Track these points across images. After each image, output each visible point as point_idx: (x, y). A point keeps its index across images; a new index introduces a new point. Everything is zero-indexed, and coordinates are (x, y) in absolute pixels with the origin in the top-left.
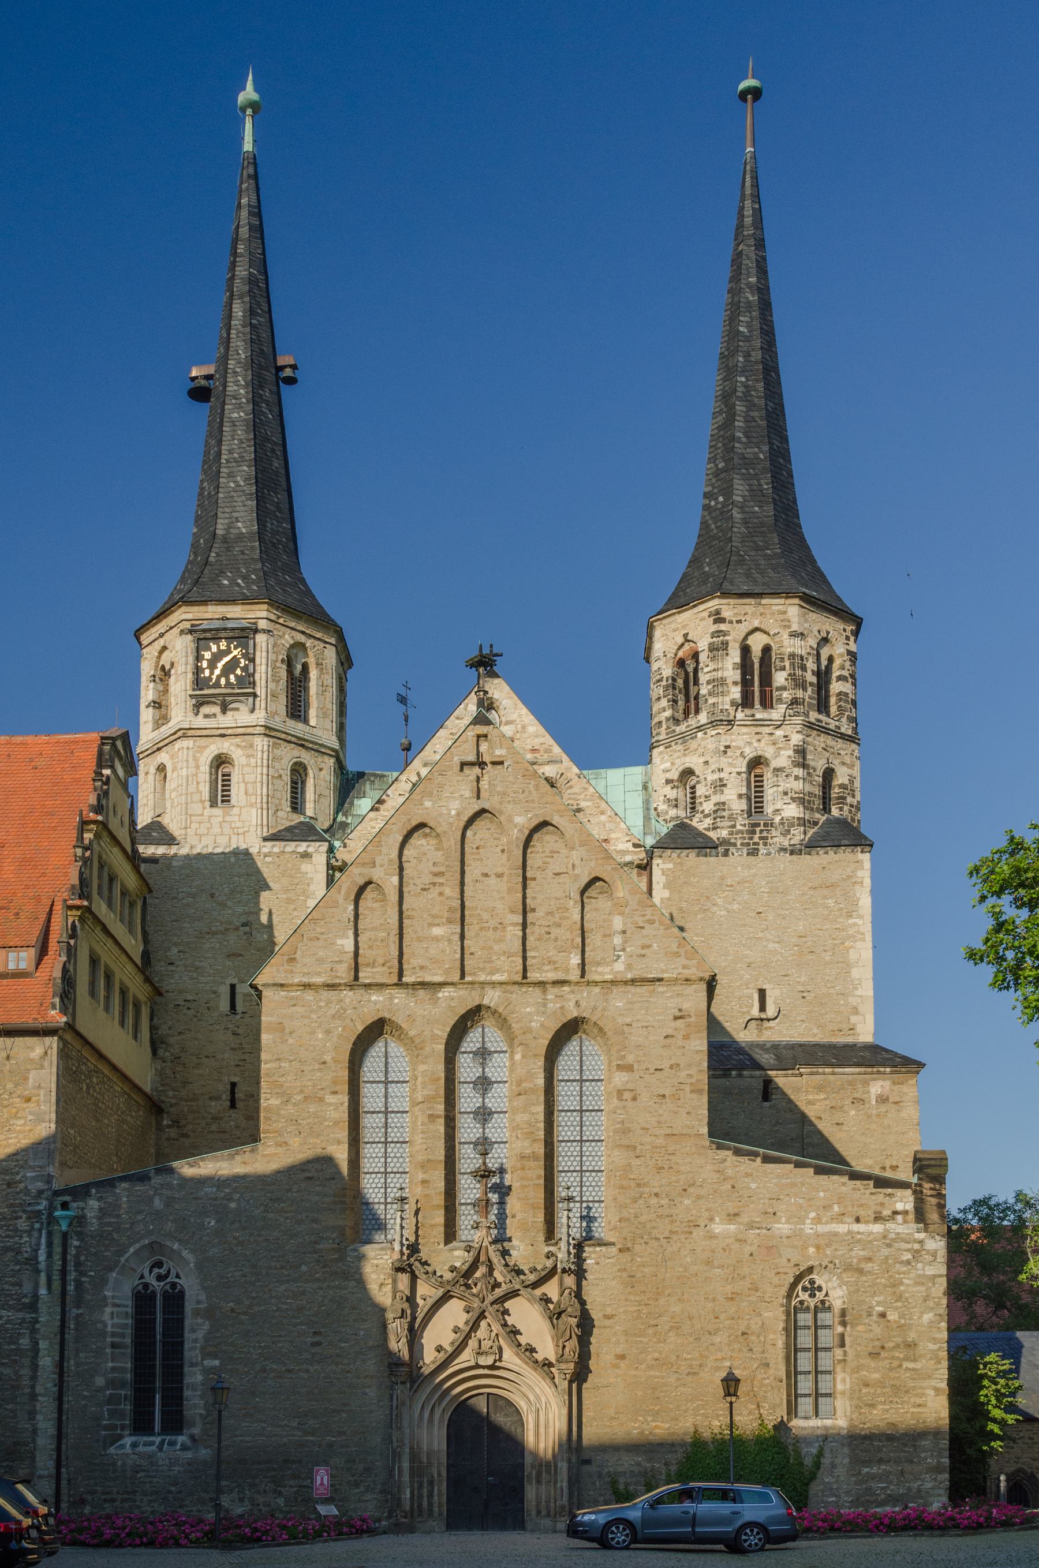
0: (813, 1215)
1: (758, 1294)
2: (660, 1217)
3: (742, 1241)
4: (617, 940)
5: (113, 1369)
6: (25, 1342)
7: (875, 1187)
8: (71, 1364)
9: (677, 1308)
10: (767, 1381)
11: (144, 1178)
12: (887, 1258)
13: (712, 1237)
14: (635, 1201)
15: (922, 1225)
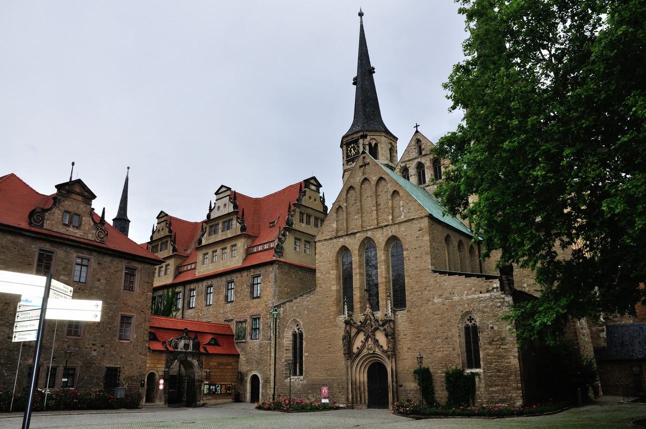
0: (466, 292)
1: (450, 323)
2: (419, 299)
3: (444, 304)
4: (401, 209)
5: (286, 357)
6: (269, 349)
7: (486, 279)
8: (277, 355)
9: (425, 330)
10: (455, 355)
11: (291, 301)
12: (492, 306)
13: (434, 304)
14: (411, 294)
15: (503, 292)
